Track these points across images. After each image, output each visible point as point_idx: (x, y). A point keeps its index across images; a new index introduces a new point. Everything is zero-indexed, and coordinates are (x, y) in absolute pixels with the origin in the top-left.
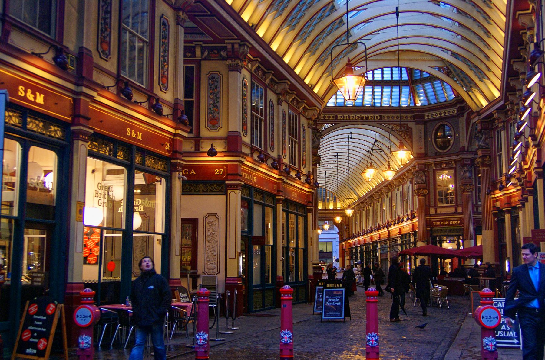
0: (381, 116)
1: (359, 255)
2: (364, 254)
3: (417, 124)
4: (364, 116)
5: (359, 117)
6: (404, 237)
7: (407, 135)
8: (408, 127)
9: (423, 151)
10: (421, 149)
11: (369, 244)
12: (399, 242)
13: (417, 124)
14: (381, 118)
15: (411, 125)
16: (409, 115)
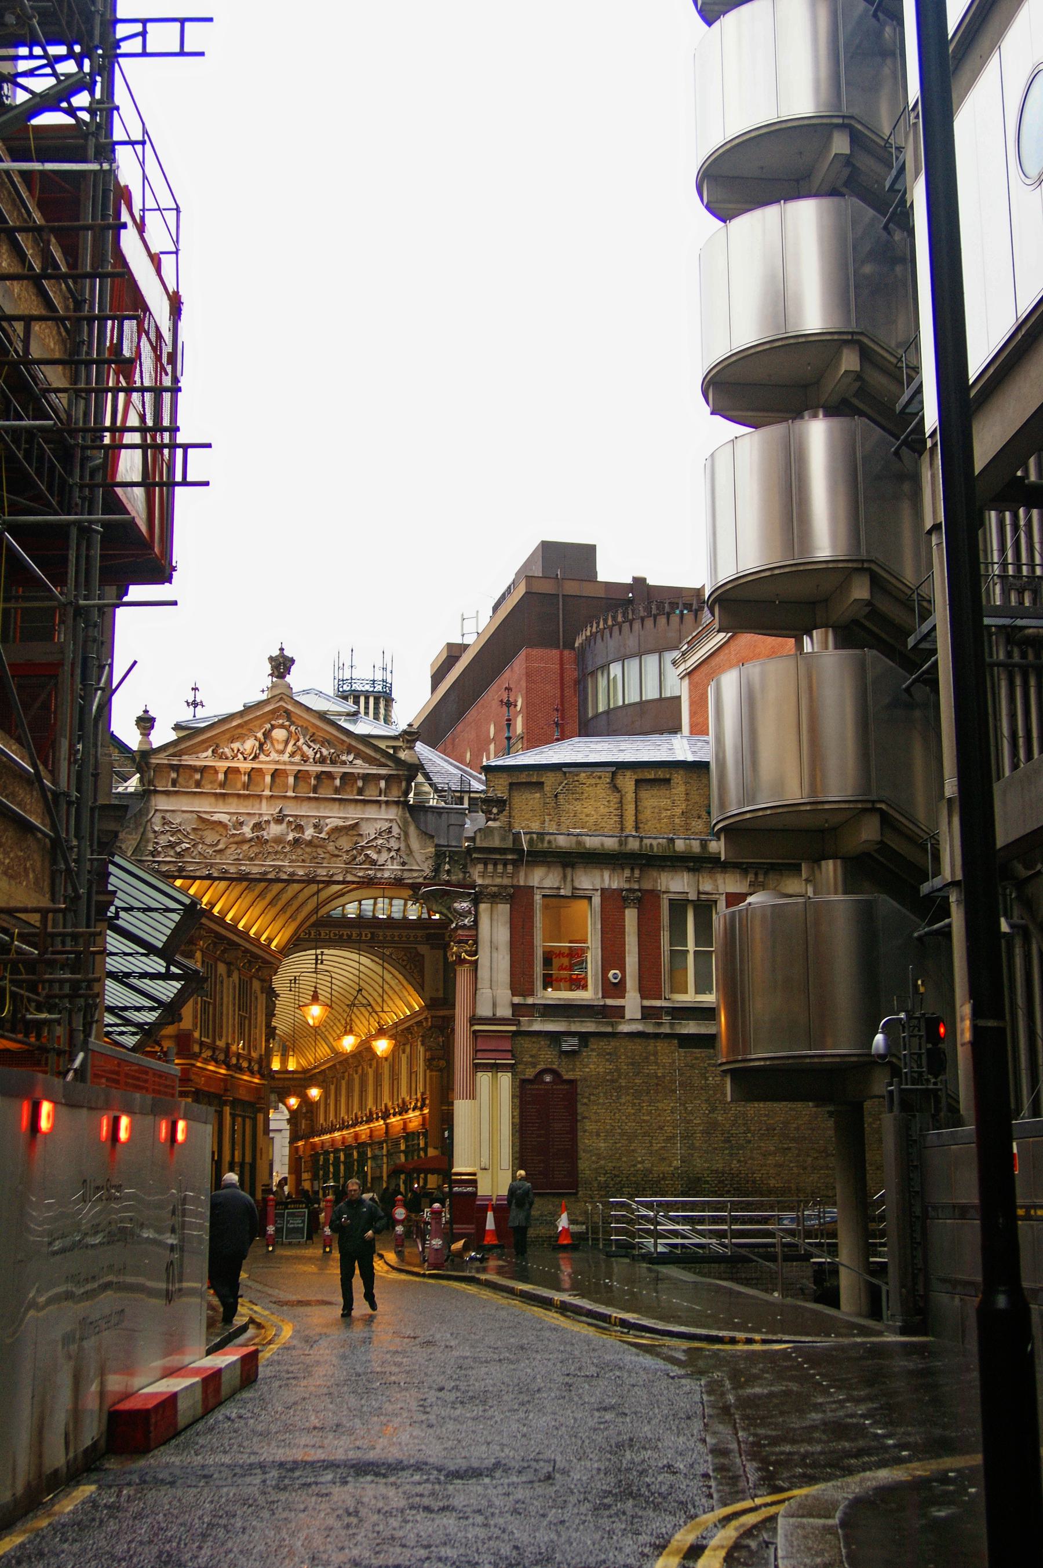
0: (372, 934)
1: (331, 1169)
2: (342, 1167)
3: (432, 948)
4: (345, 932)
5: (335, 935)
6: (410, 1138)
7: (416, 966)
8: (418, 954)
9: (441, 995)
10: (437, 990)
11: (350, 1147)
12: (403, 1147)
13: (432, 948)
14: (372, 938)
15: (423, 949)
16: (420, 933)
